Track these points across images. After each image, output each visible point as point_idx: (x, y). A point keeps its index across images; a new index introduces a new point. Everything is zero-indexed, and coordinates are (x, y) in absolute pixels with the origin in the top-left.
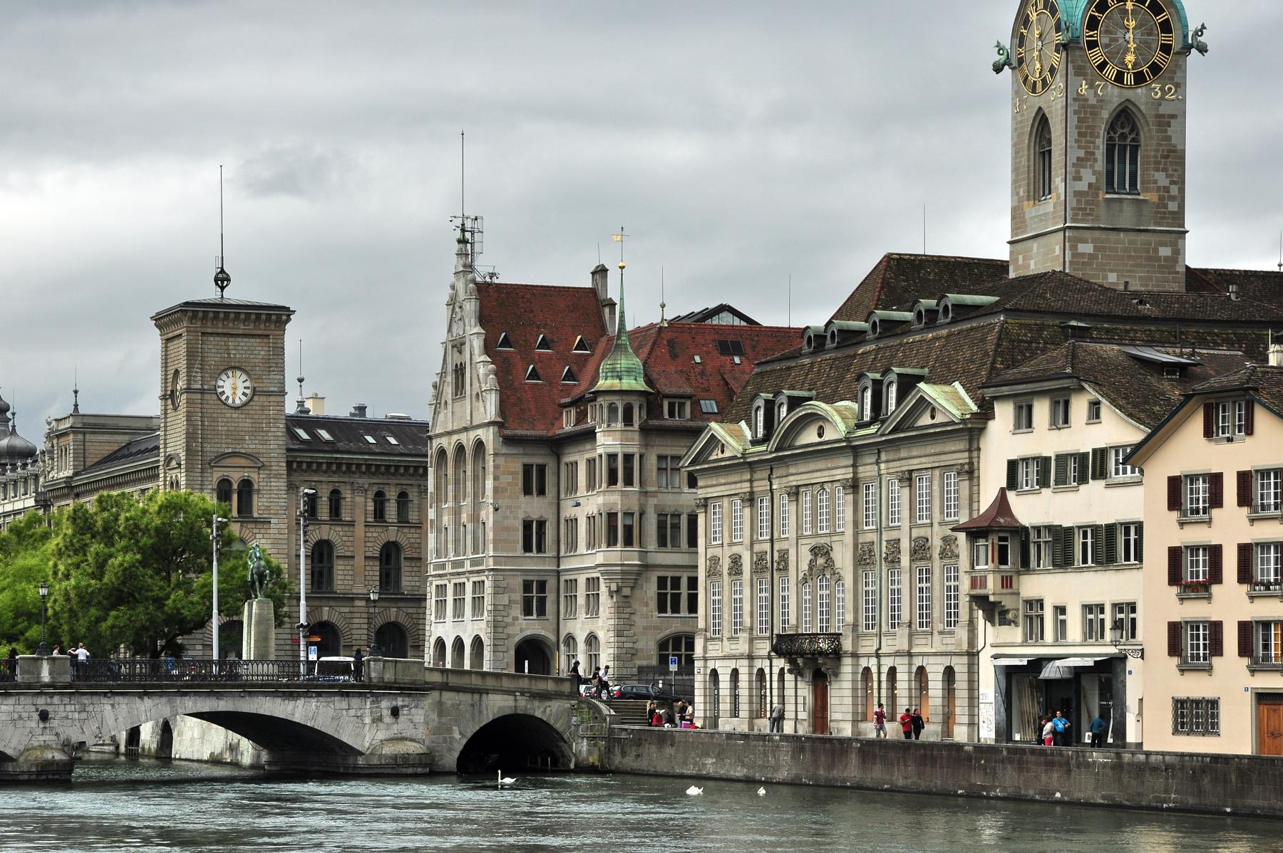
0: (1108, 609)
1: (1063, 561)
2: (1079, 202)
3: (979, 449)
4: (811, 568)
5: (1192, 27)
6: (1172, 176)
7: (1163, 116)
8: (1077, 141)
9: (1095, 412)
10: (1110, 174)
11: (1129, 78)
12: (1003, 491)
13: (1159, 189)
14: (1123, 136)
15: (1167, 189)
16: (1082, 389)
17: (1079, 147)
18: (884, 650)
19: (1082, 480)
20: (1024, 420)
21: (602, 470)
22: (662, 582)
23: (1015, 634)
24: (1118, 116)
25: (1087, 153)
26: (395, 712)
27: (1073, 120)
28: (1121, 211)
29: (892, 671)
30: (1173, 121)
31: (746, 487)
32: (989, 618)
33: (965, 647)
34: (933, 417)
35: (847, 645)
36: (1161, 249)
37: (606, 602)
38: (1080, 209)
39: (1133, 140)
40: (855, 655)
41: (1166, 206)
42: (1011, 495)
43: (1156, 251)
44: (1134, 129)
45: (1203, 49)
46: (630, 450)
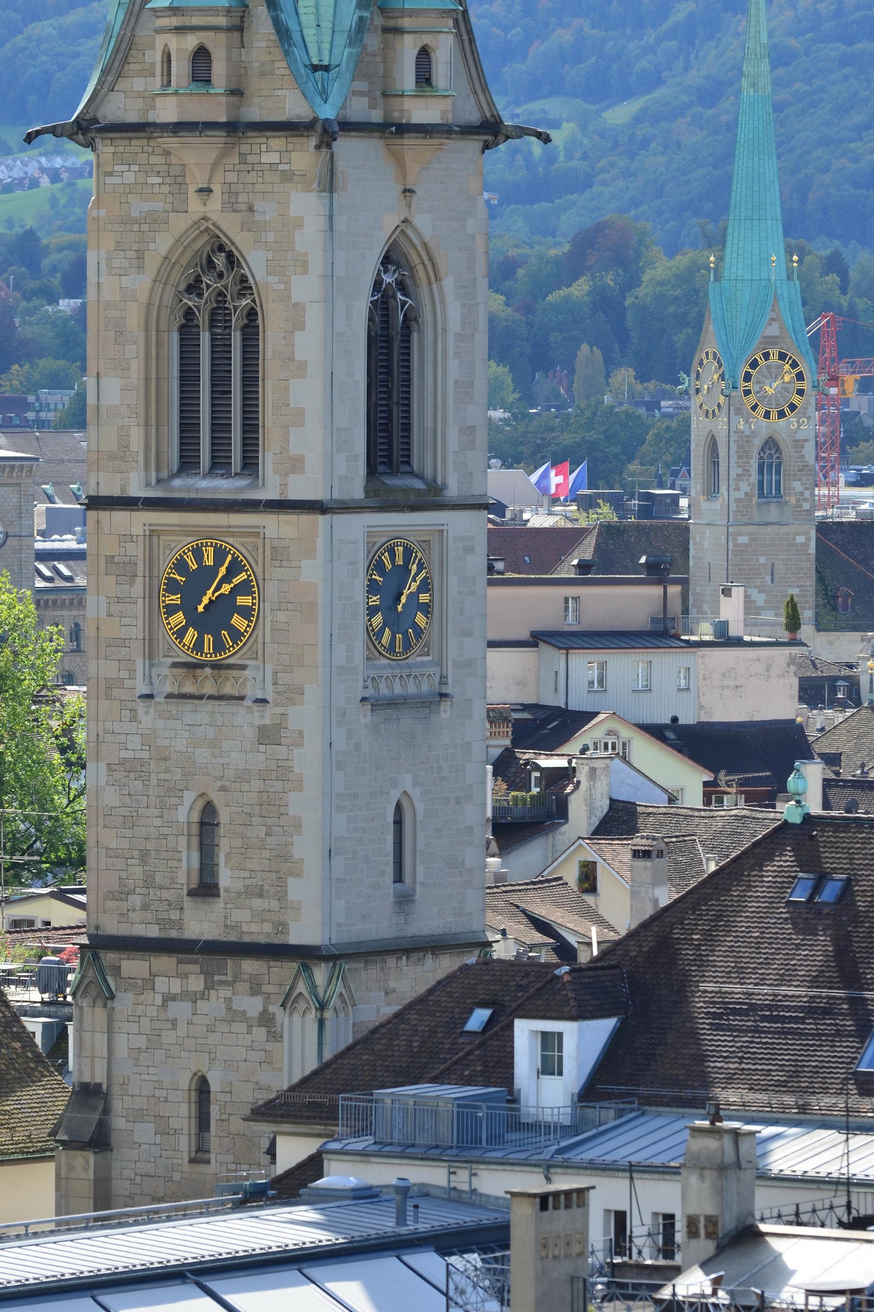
2: (738, 506)
6: (805, 484)
7: (798, 441)
8: (736, 463)
10: (761, 483)
11: (774, 414)
13: (796, 494)
14: (771, 456)
15: (801, 494)
17: (738, 467)
24: (767, 442)
25: (744, 470)
27: (734, 447)
28: (768, 511)
30: (806, 444)
36: (797, 537)
38: (739, 511)
39: (778, 458)
41: (801, 506)
43: (794, 539)
44: (778, 449)
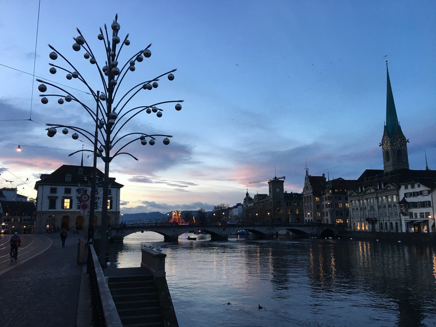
0: (424, 213)
1: (416, 207)
3: (399, 192)
4: (370, 209)
5: (407, 139)
9: (419, 186)
12: (404, 198)
16: (416, 183)
18: (384, 220)
19: (418, 195)
20: (406, 188)
21: (327, 198)
22: (336, 212)
23: (408, 217)
26: (312, 229)
29: (386, 223)
31: (358, 199)
32: (403, 215)
33: (399, 219)
34: (390, 188)
35: (378, 219)
37: (329, 215)
40: (379, 221)
42: (405, 198)
45: (409, 142)
46: (331, 196)
